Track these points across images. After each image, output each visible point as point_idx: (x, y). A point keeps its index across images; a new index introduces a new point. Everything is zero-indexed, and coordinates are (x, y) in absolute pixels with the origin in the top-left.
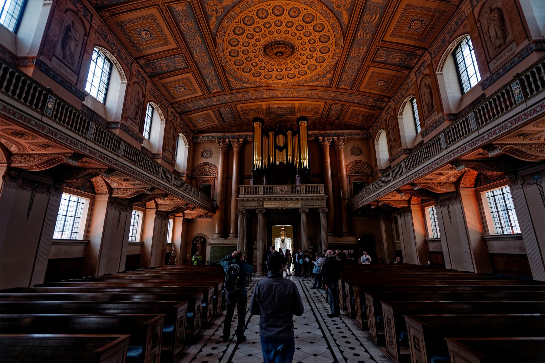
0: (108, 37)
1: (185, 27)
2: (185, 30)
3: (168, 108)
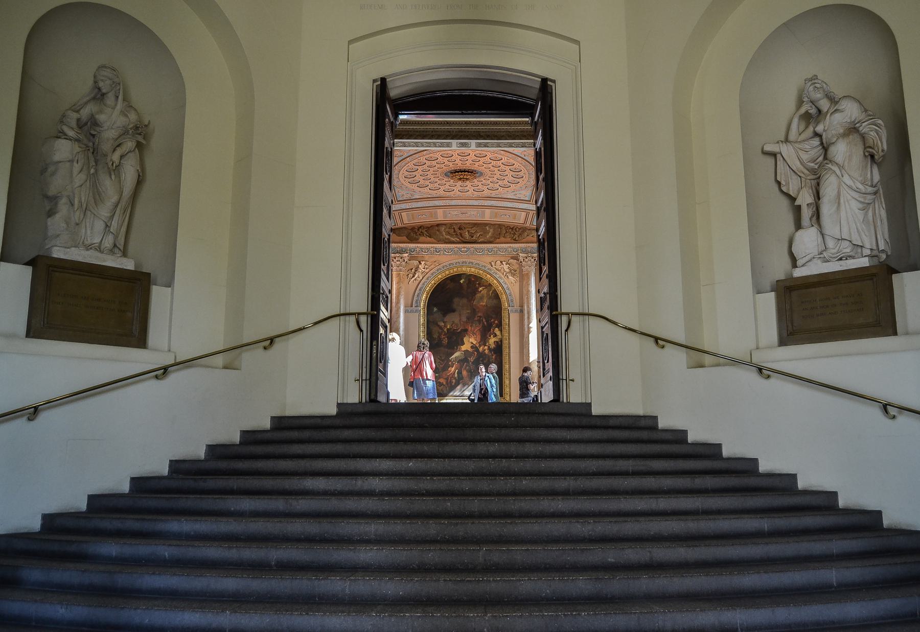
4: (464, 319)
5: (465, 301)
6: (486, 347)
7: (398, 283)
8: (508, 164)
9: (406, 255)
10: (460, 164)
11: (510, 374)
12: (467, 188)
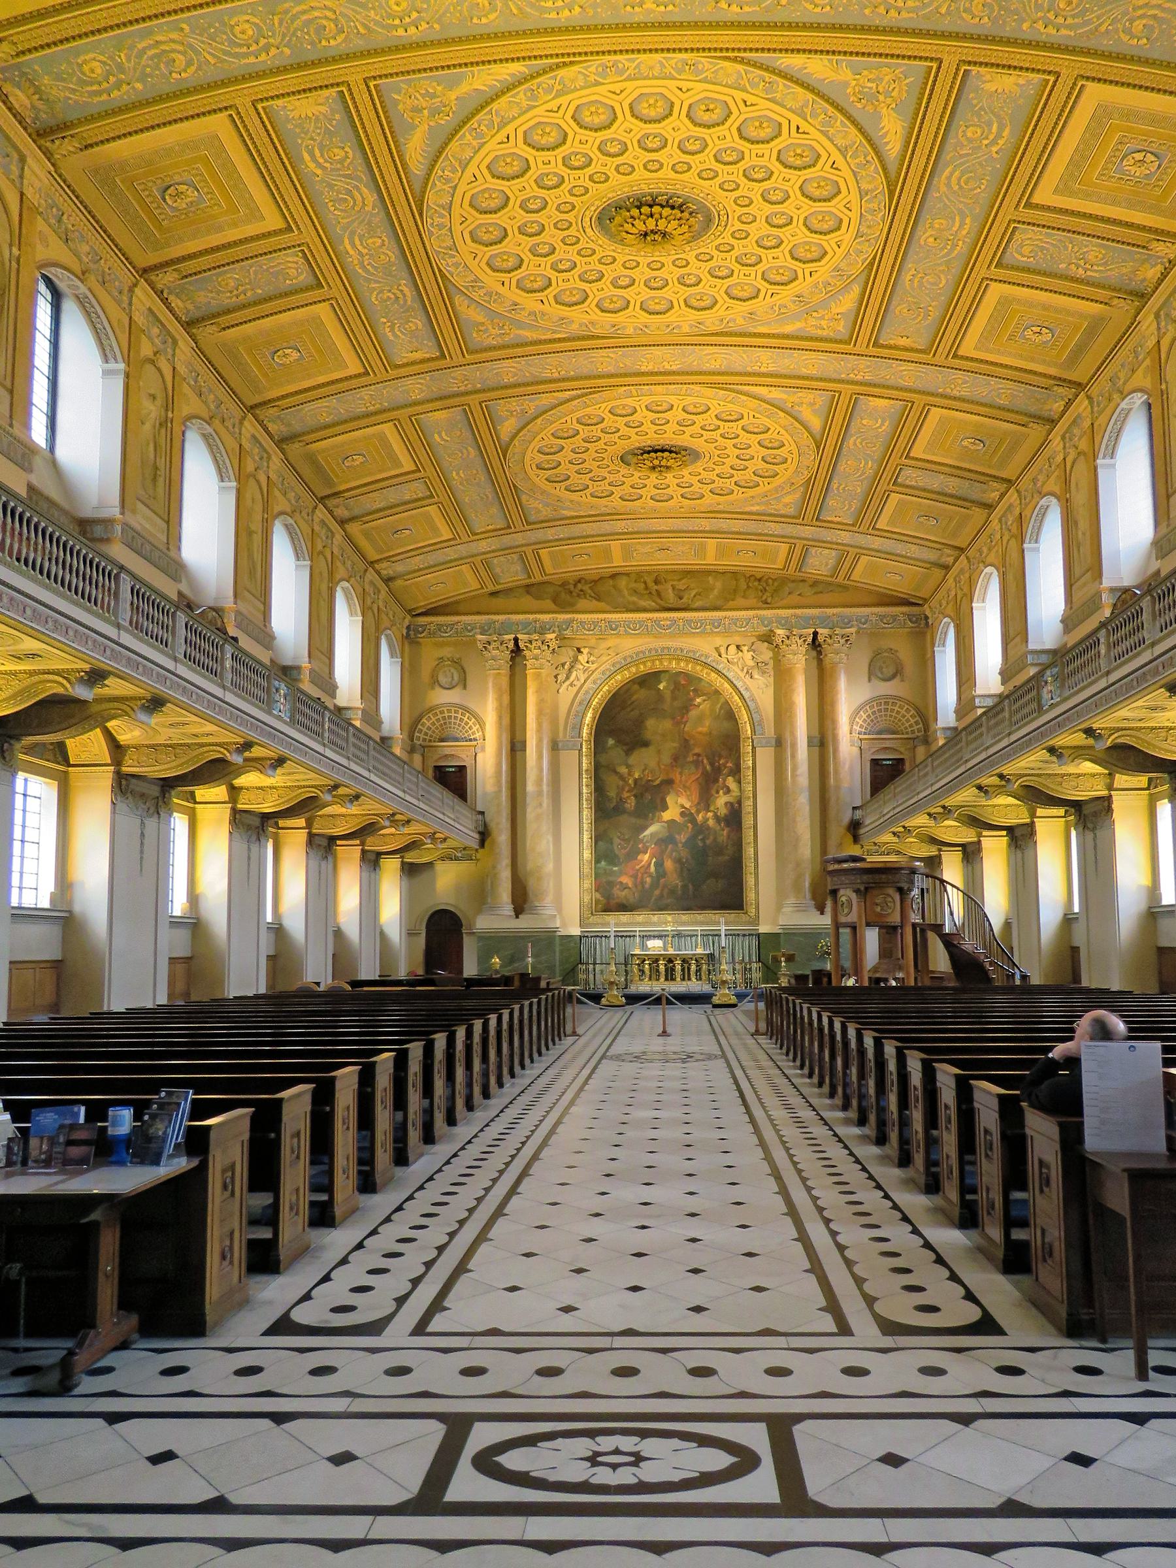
0: (65, 217)
1: (319, 165)
2: (319, 172)
3: (241, 423)
4: (666, 759)
5: (667, 724)
6: (710, 814)
8: (756, 430)
9: (553, 636)
10: (651, 435)
12: (669, 491)
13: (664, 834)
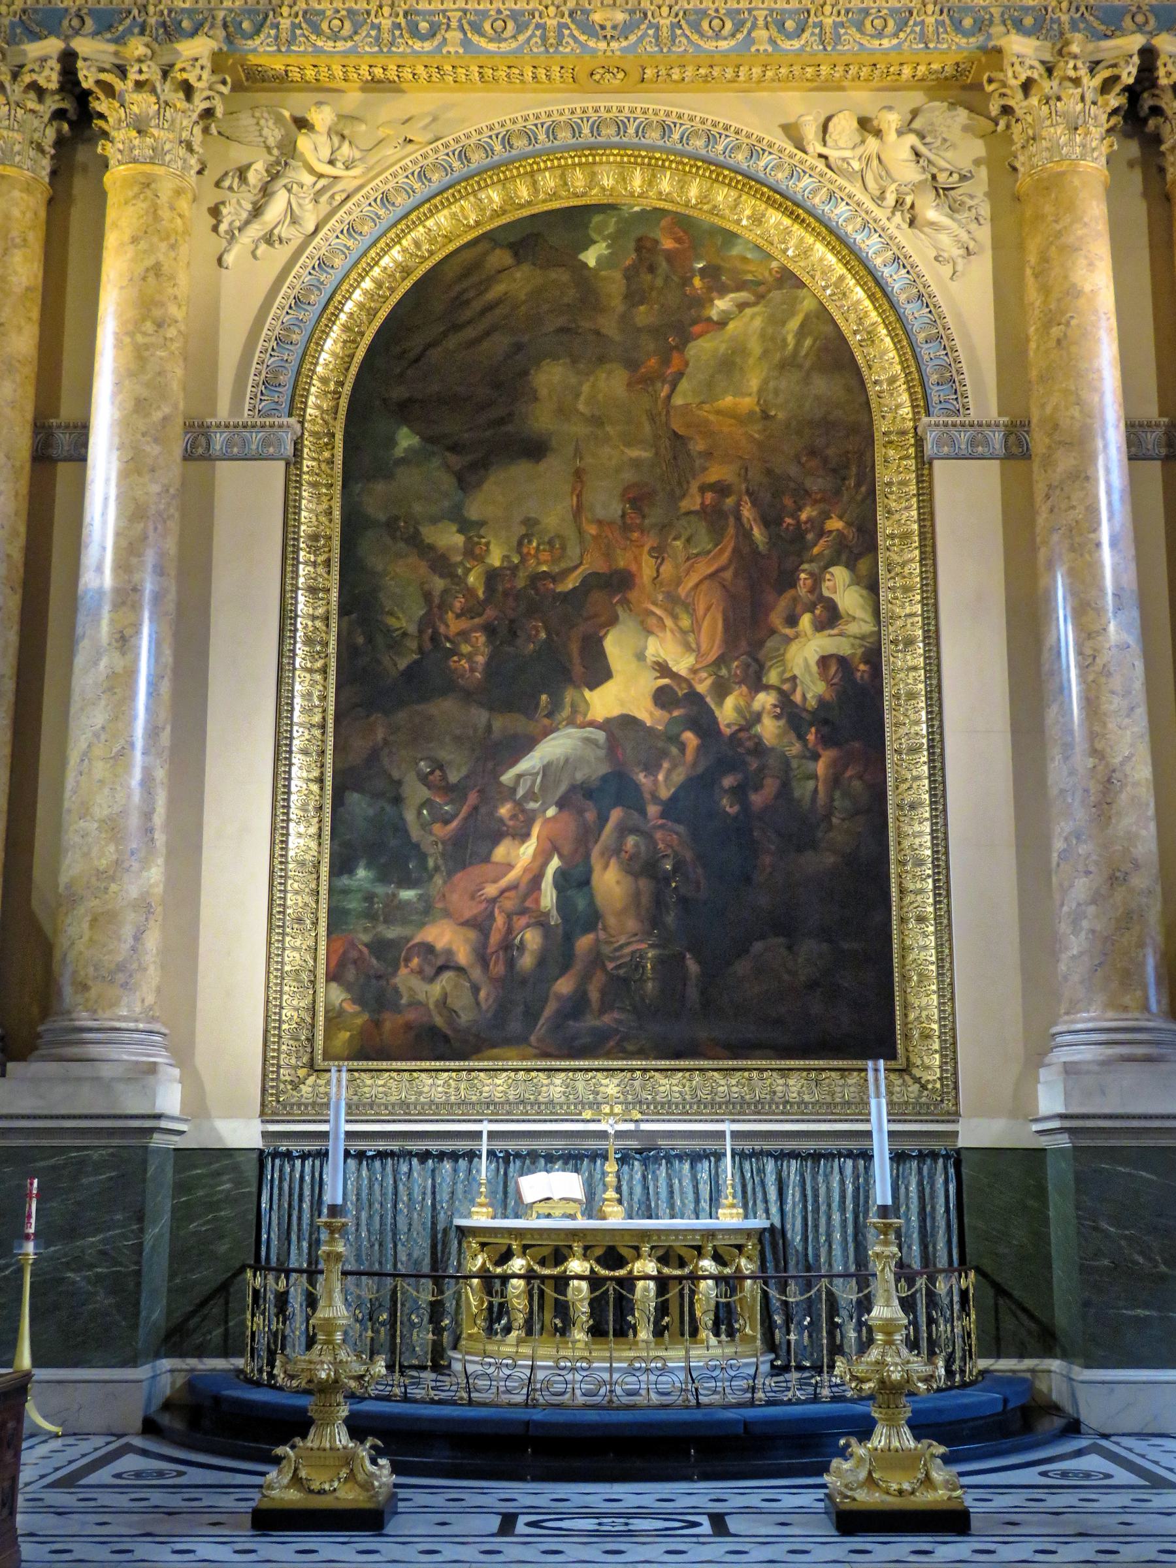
6: (765, 700)
7: (135, 240)
11: (942, 891)
13: (595, 768)
